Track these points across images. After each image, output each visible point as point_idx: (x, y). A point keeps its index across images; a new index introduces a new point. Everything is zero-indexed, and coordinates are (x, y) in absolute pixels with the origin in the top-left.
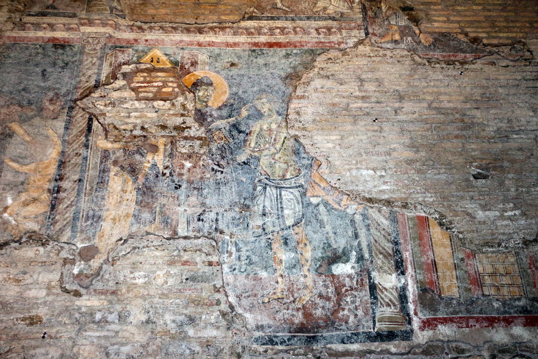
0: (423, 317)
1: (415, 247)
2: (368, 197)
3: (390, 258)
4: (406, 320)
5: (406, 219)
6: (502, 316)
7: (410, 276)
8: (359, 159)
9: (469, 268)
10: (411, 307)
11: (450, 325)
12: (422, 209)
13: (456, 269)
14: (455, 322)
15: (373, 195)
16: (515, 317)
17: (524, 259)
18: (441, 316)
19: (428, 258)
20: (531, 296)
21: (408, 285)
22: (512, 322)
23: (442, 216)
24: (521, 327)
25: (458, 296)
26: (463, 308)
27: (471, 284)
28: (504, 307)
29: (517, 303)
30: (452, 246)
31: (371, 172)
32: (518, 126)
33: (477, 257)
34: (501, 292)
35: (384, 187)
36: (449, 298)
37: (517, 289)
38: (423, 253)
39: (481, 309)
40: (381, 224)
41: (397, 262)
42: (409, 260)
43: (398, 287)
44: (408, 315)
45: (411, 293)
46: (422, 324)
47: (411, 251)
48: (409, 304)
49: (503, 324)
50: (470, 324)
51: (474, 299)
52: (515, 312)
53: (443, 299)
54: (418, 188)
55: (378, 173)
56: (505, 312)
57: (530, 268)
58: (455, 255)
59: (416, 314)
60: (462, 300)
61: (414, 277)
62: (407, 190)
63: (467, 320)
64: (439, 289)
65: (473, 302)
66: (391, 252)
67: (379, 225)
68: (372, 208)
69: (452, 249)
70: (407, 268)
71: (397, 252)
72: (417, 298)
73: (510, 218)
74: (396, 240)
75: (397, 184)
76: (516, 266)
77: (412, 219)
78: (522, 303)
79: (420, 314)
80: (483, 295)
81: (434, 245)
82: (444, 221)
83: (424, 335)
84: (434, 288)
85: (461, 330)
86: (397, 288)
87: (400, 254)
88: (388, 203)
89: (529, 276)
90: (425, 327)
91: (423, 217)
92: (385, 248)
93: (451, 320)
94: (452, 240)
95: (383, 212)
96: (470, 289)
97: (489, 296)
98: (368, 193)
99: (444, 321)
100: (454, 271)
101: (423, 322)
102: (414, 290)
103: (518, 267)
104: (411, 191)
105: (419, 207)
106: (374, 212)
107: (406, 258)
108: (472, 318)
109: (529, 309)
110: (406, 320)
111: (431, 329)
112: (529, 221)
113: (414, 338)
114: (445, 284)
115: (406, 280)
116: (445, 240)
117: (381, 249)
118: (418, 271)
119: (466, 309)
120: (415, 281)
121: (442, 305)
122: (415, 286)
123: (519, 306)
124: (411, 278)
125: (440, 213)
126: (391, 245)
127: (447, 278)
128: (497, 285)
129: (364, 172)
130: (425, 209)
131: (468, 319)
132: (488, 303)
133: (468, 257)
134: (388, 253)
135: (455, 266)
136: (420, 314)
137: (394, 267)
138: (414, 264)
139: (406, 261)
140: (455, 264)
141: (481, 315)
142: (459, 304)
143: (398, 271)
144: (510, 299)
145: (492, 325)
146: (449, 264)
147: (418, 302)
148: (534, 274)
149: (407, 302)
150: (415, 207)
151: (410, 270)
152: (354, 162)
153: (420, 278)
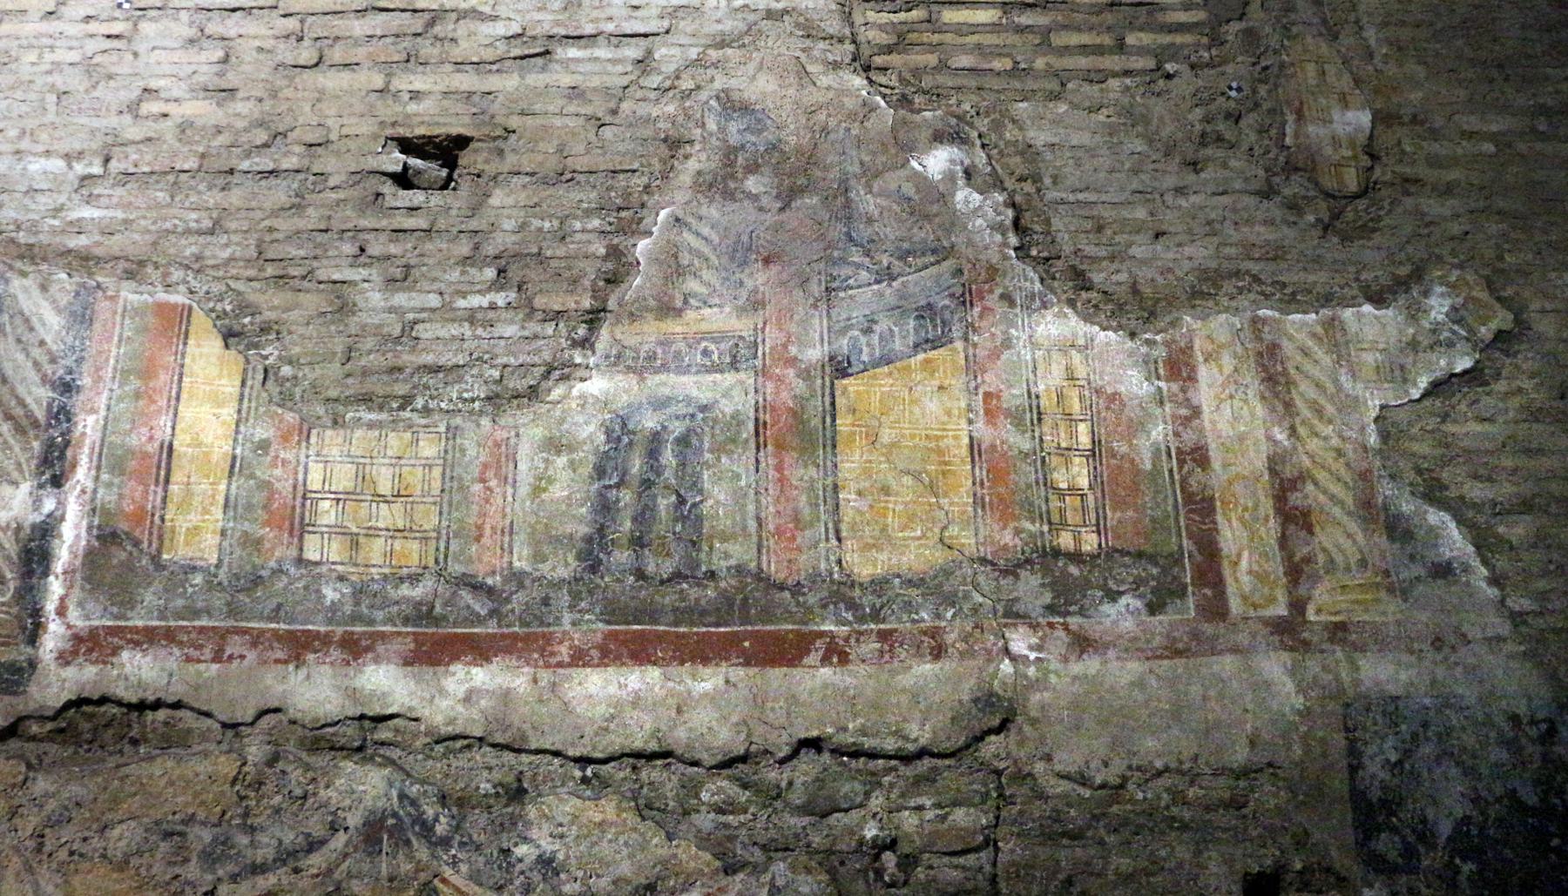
0: (80, 623)
1: (120, 399)
2: (22, 241)
3: (31, 433)
4: (24, 628)
5: (120, 311)
6: (340, 630)
7: (76, 493)
8: (30, 124)
9: (278, 472)
10: (55, 587)
11: (163, 652)
12: (185, 282)
13: (231, 474)
14: (181, 644)
15: (41, 237)
16: (383, 636)
17: (472, 452)
18: (140, 623)
19: (151, 438)
20: (456, 568)
21: (62, 518)
22: (368, 649)
23: (244, 307)
24: (392, 667)
25: (214, 561)
26: (219, 600)
27: (267, 523)
28: (357, 604)
29: (405, 590)
30: (241, 400)
31: (57, 164)
32: (595, 21)
33: (313, 440)
34: (362, 554)
35: (87, 212)
36: (182, 566)
37: (415, 546)
38: (140, 418)
39: (279, 606)
40: (37, 326)
41: (50, 445)
42: (88, 441)
43: (27, 524)
44: (37, 612)
45: (65, 547)
46: (68, 646)
47: (103, 413)
48: (52, 578)
49: (336, 654)
50: (228, 652)
51: (264, 573)
52: (390, 620)
53: (164, 568)
54: (194, 216)
55: (80, 169)
56: (356, 618)
57: (483, 481)
58: (242, 428)
59: (61, 611)
60: (223, 575)
61: (87, 497)
62: (155, 223)
63: (223, 637)
64: (161, 538)
65: (257, 581)
66: (40, 415)
67: (32, 329)
68: (24, 274)
69: (239, 411)
70: (74, 466)
71: (61, 415)
72: (78, 563)
73: (471, 317)
74: (68, 378)
75: (130, 203)
76: (437, 472)
77: (138, 312)
78: (417, 592)
79: (74, 615)
80: (300, 561)
81: (184, 396)
82: (247, 320)
83: (64, 680)
84: (142, 532)
85: (192, 668)
86: (19, 528)
87: (69, 420)
88: (84, 261)
89: (469, 504)
90: (75, 653)
91: (175, 306)
92: (29, 400)
93: (170, 636)
94: (249, 383)
95: (54, 289)
96: (258, 542)
97: (317, 564)
98: (29, 231)
99: (147, 638)
100: (225, 481)
101: (77, 639)
102: (78, 537)
103: (444, 474)
104: (168, 225)
105: (177, 275)
106: (26, 290)
107: (84, 434)
108: (245, 631)
109: (438, 609)
110: (24, 628)
111: (96, 662)
112: (534, 327)
113: (33, 689)
114: (180, 521)
115: (61, 504)
116: (224, 382)
117: (13, 403)
118: (105, 477)
119: (228, 604)
120: (87, 508)
121: (157, 586)
122: (84, 523)
123: (407, 600)
124: (78, 497)
125: (239, 293)
126: (45, 393)
127: (196, 501)
128: (355, 530)
129: (36, 166)
130: (193, 283)
131: (223, 635)
132: (306, 588)
133: (285, 438)
134: (29, 415)
135: (233, 466)
136: (74, 615)
137: (34, 462)
138: (100, 455)
139: (80, 445)
140: (234, 458)
141: (273, 626)
142: (211, 585)
143: (43, 473)
144: (385, 577)
145: (297, 658)
146: (215, 458)
147: (78, 576)
148: (487, 501)
149: (46, 574)
150: (166, 275)
151: (82, 475)
152: (13, 133)
153: (108, 498)
